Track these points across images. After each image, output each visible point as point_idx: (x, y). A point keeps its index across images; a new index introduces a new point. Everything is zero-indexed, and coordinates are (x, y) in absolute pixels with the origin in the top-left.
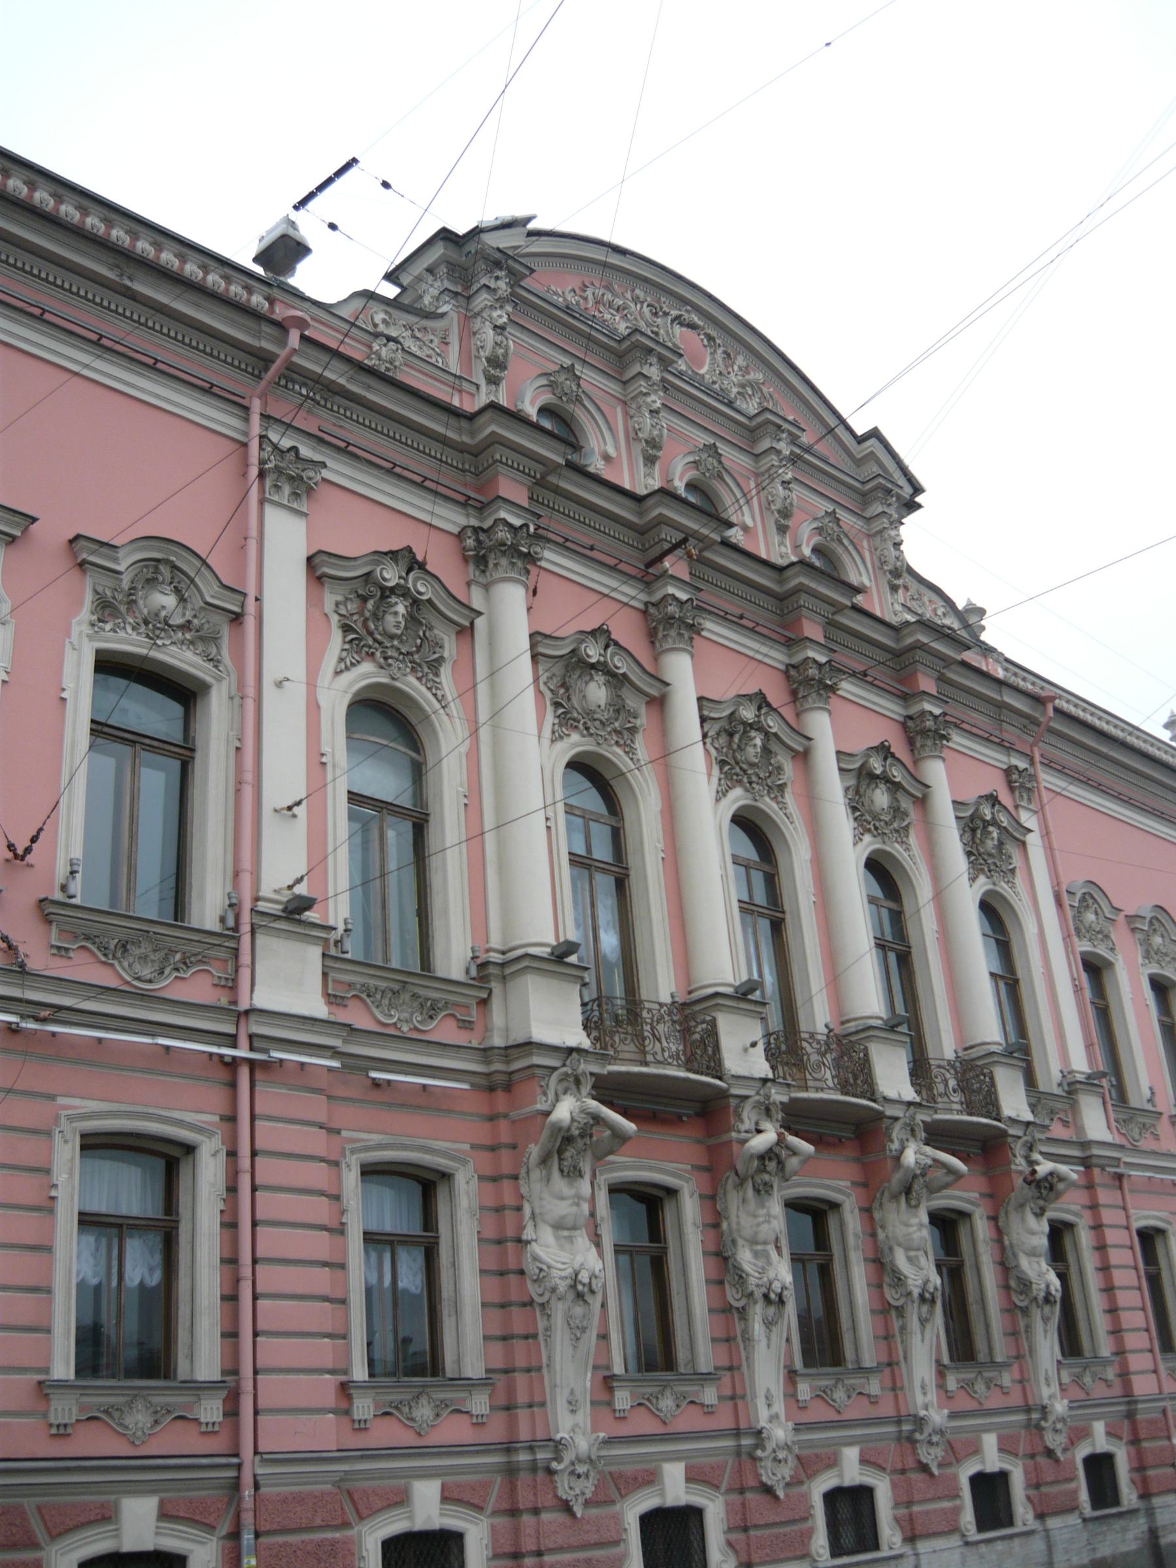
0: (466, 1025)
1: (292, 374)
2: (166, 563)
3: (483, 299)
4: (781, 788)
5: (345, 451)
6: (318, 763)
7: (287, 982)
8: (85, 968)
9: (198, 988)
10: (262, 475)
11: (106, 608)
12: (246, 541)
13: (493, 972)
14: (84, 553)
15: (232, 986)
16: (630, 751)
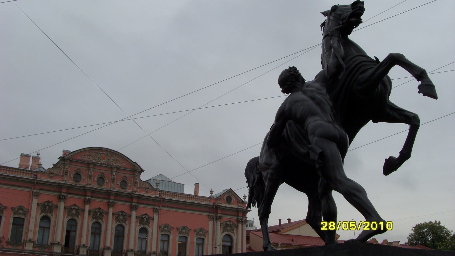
0: (49, 249)
1: (37, 183)
2: (21, 208)
3: (66, 164)
4: (102, 219)
5: (43, 190)
6: (36, 224)
7: (29, 247)
8: (10, 247)
9: (20, 248)
10: (33, 195)
11: (14, 213)
12: (31, 204)
13: (53, 244)
14: (12, 208)
15: (23, 247)
16: (78, 217)
